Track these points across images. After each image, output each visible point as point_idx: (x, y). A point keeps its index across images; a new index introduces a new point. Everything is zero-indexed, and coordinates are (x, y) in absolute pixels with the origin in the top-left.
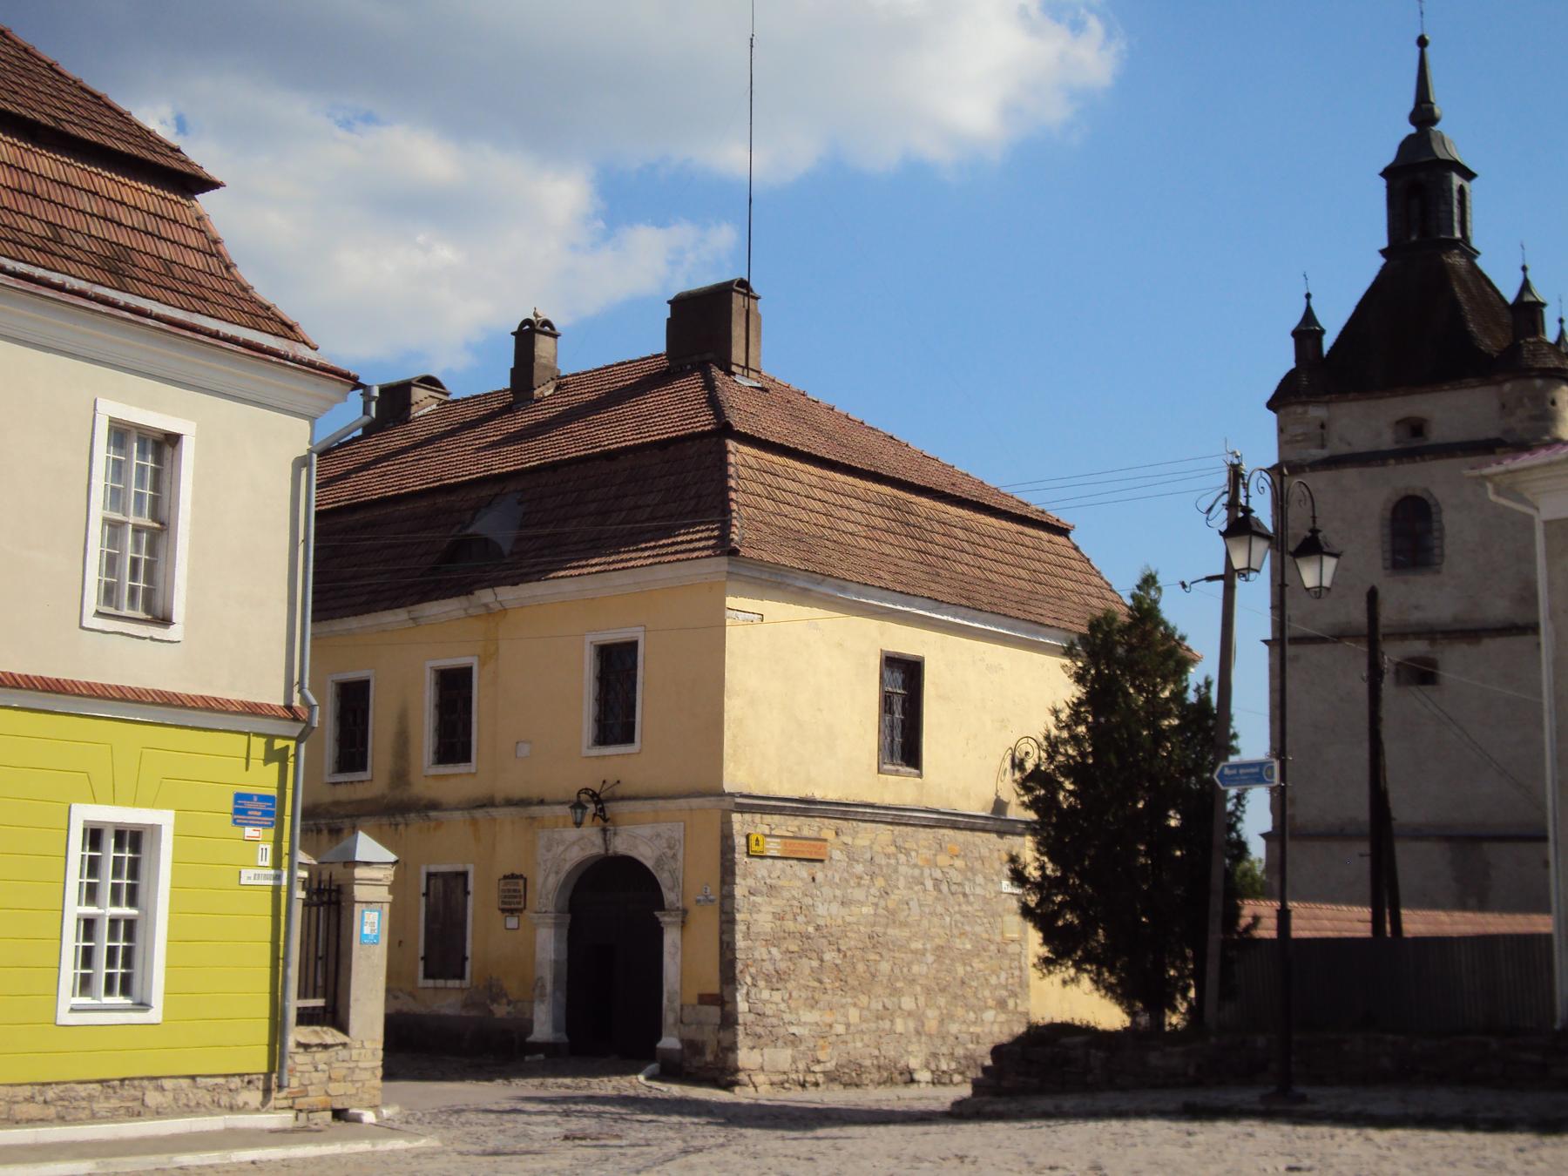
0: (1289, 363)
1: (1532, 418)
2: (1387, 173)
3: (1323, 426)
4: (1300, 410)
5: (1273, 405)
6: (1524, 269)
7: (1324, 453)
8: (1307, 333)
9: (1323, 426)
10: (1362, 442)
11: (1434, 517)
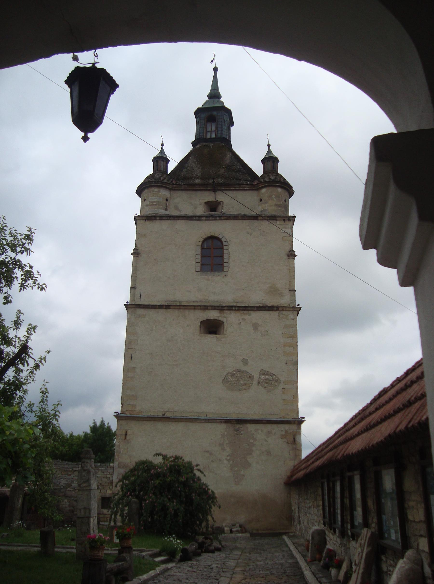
0: (150, 171)
1: (276, 205)
2: (198, 113)
3: (167, 200)
4: (156, 190)
5: (140, 191)
6: (269, 145)
7: (167, 213)
8: (160, 160)
9: (167, 200)
10: (187, 210)
11: (225, 248)
